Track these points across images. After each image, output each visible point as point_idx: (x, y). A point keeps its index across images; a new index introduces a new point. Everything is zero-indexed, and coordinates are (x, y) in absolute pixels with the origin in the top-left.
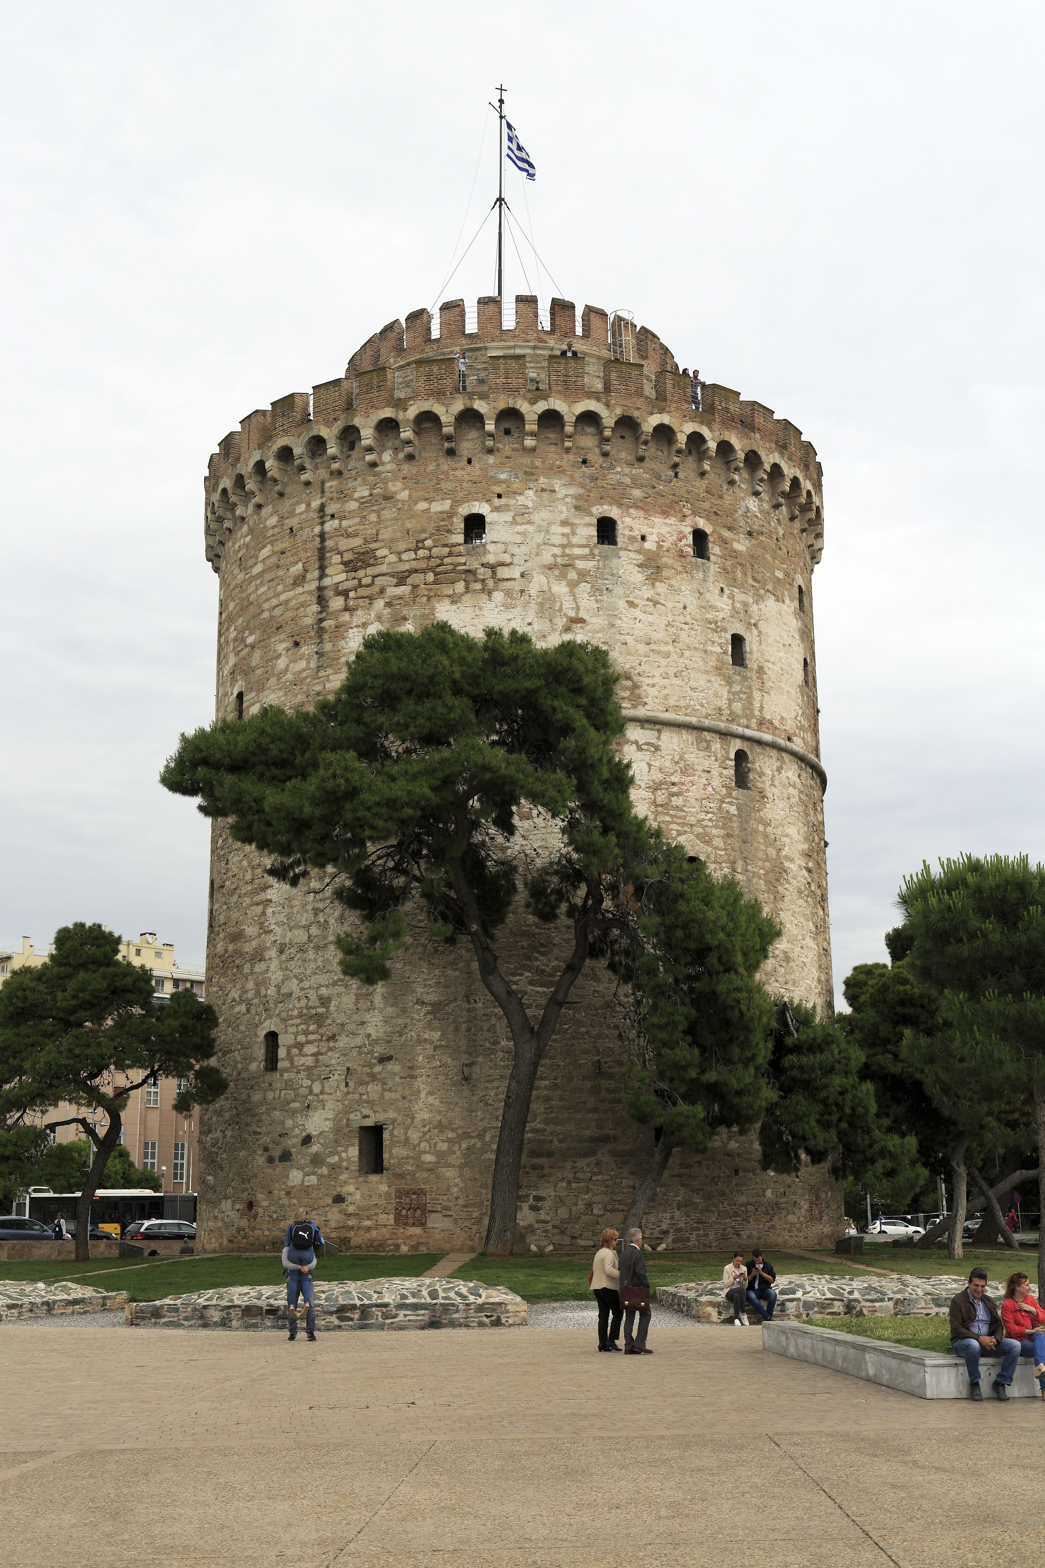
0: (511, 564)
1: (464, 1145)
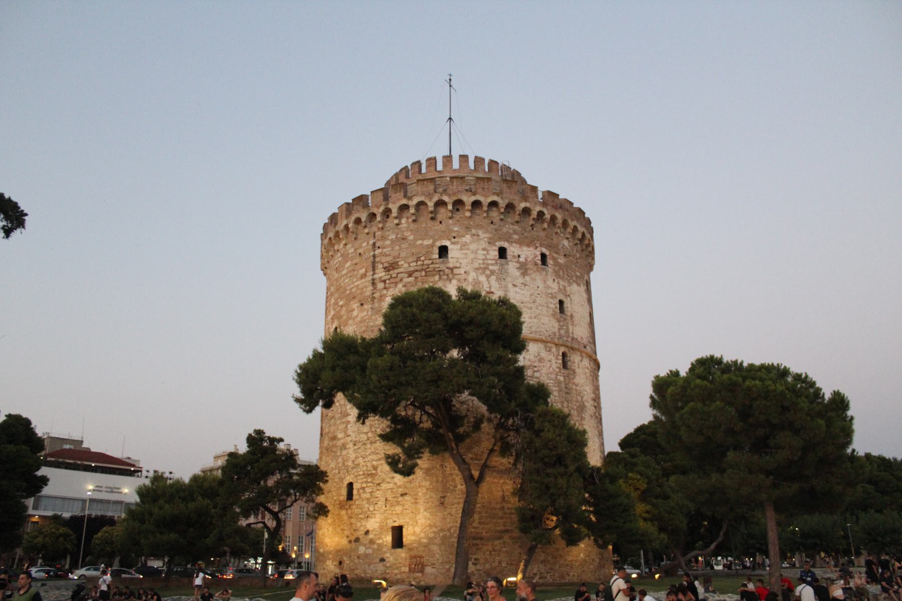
0: (460, 267)
1: (441, 535)
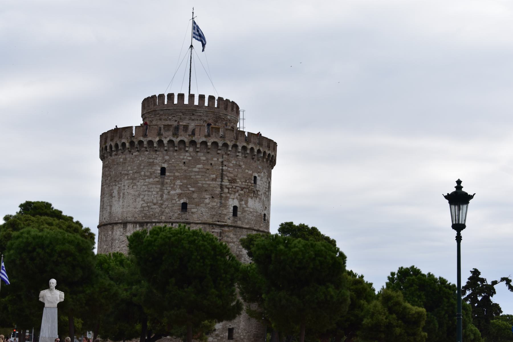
1: (248, 334)
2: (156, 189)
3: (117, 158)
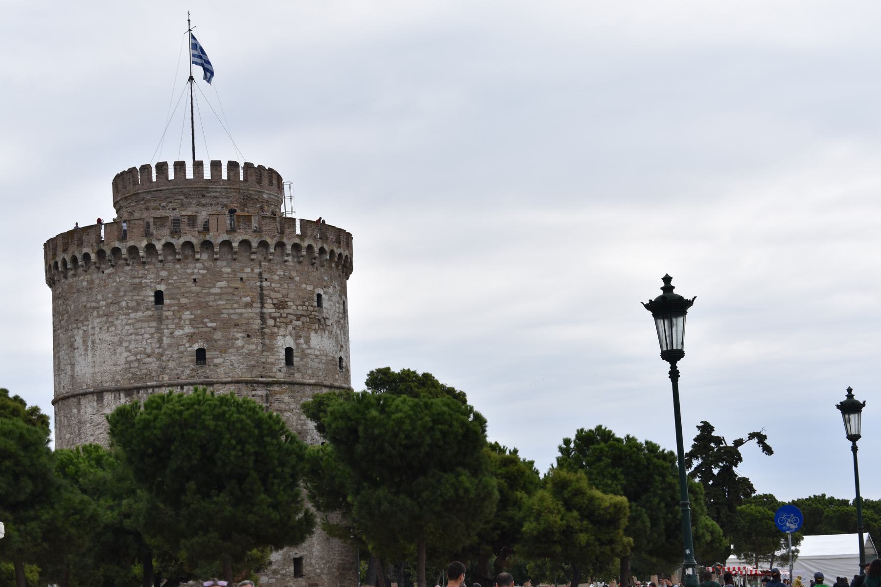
1: (328, 566)
2: (149, 329)
3: (76, 282)
